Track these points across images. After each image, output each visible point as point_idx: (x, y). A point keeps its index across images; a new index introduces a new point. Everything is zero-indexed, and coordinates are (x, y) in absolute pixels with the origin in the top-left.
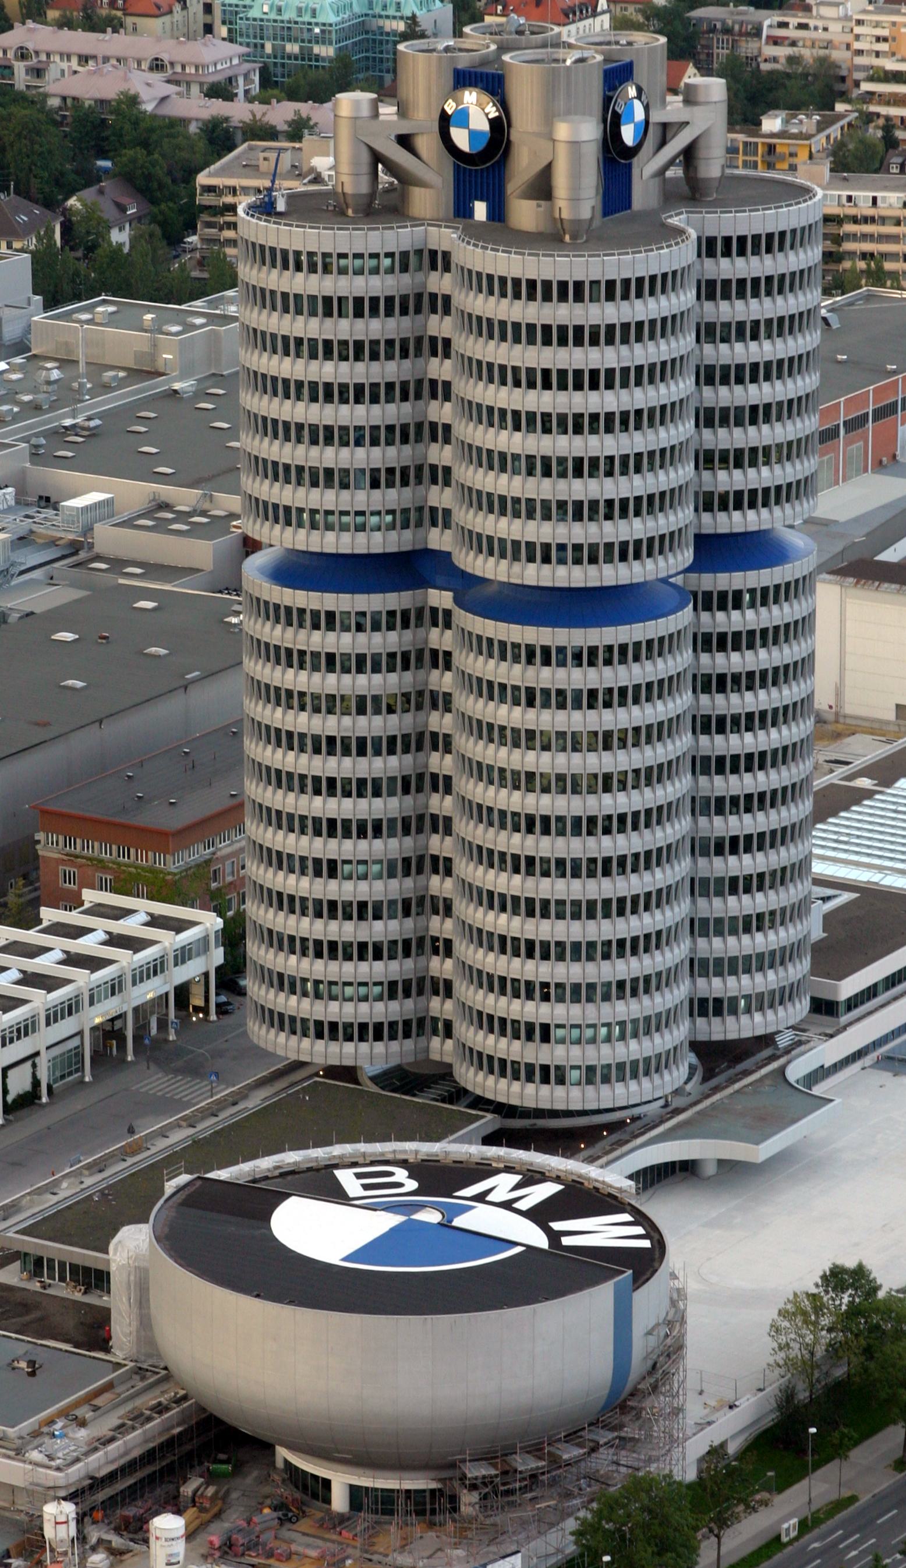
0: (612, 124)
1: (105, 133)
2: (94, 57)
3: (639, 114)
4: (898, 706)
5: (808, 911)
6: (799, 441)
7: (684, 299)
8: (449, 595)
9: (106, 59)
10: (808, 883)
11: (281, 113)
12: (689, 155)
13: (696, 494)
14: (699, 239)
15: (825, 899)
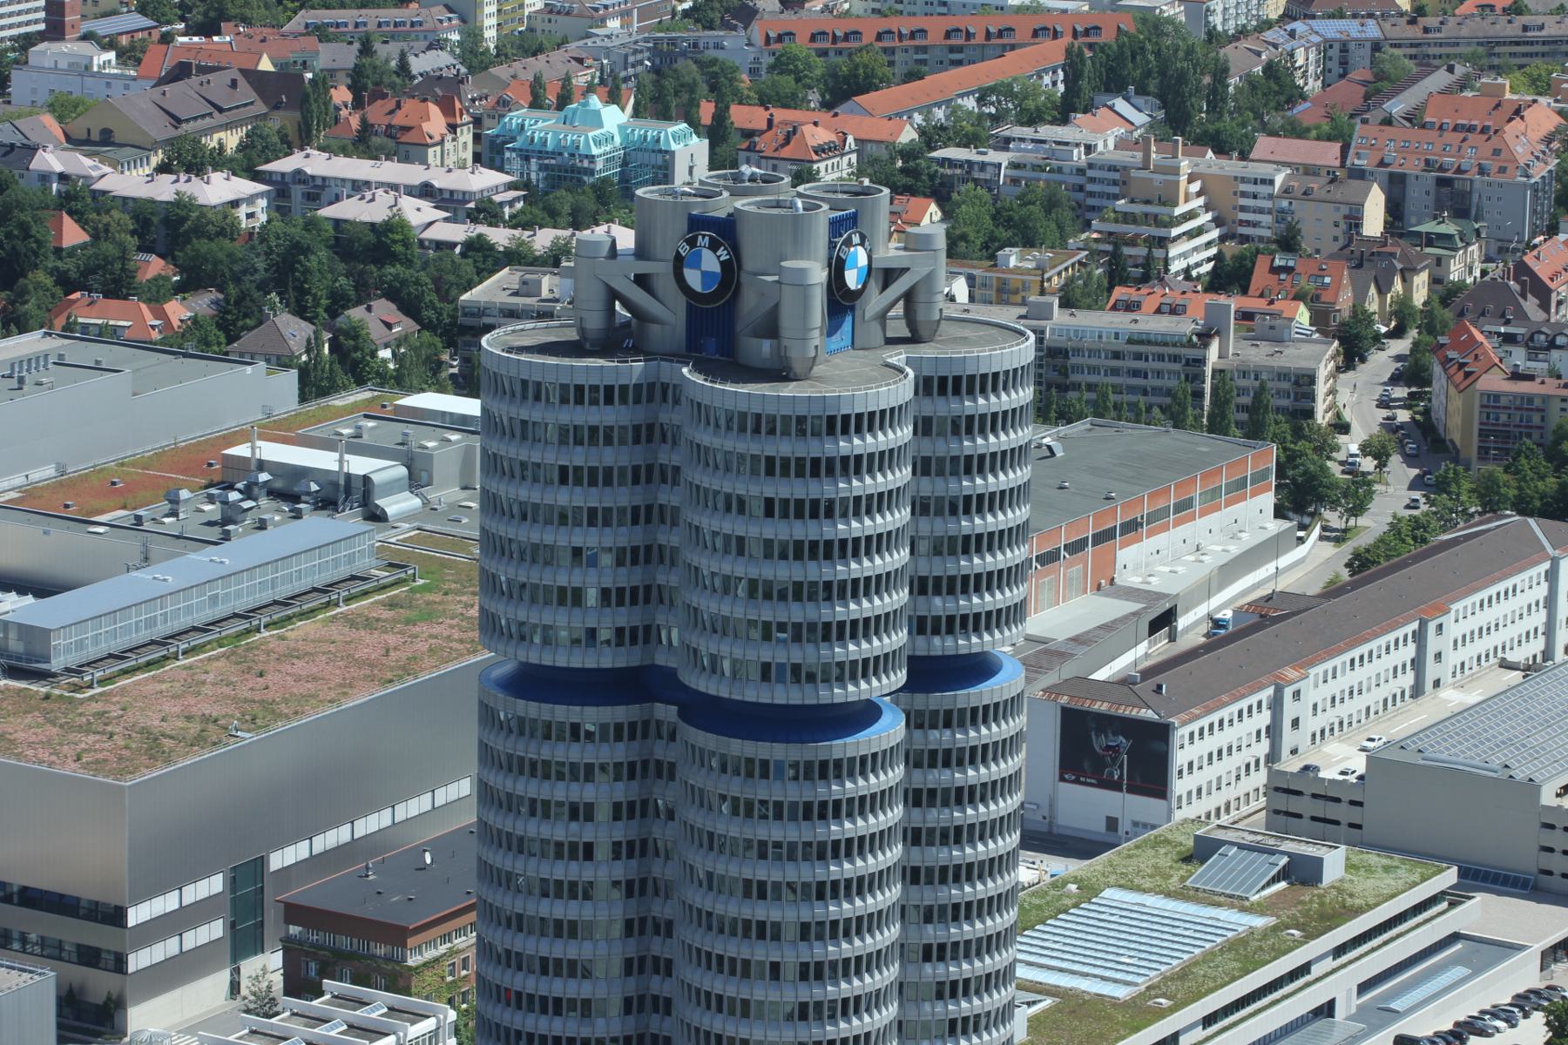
0: (837, 268)
1: (377, 253)
2: (367, 184)
3: (862, 260)
4: (1108, 818)
5: (1011, 1016)
6: (1010, 569)
7: (903, 434)
8: (674, 709)
9: (380, 185)
10: (1011, 989)
11: (543, 239)
12: (909, 297)
13: (910, 617)
14: (916, 377)
15: (1029, 1004)
